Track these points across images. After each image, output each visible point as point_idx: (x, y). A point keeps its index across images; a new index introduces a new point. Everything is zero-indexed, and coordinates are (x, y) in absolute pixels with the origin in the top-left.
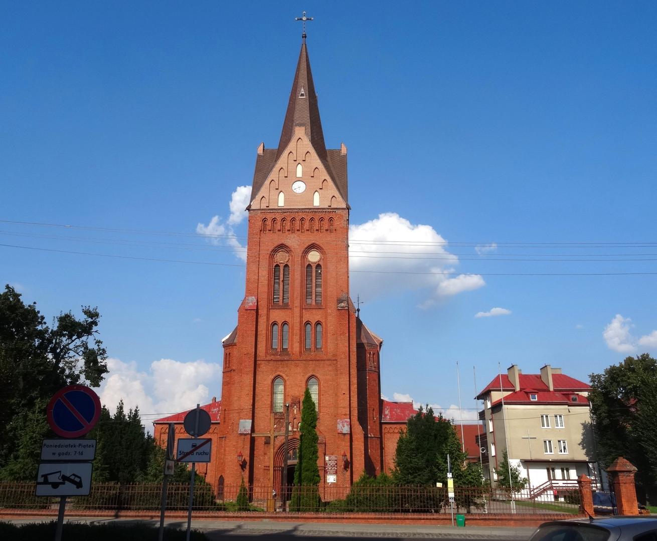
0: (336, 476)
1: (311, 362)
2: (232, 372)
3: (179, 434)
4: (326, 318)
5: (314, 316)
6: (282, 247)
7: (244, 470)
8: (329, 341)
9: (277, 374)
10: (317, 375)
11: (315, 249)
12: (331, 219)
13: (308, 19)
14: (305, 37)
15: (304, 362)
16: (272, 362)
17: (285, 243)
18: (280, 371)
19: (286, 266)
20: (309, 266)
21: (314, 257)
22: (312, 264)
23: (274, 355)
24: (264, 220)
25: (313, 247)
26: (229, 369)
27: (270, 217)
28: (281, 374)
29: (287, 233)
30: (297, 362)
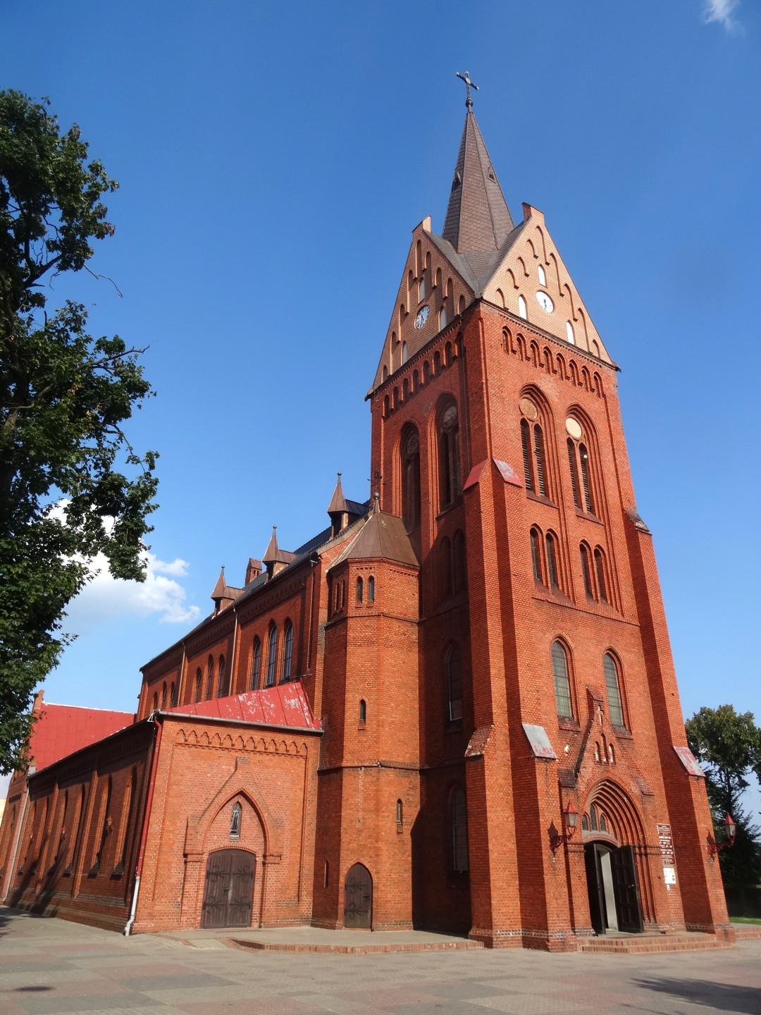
0: (673, 869)
2: (382, 618)
3: (220, 752)
4: (610, 540)
5: (596, 538)
6: (533, 392)
7: (554, 853)
8: (623, 587)
9: (558, 632)
10: (616, 649)
11: (575, 417)
13: (472, 85)
14: (467, 104)
15: (594, 617)
16: (546, 606)
18: (562, 629)
19: (537, 428)
20: (570, 442)
21: (574, 429)
22: (574, 441)
24: (506, 331)
25: (577, 412)
26: (374, 611)
27: (515, 329)
28: (564, 634)
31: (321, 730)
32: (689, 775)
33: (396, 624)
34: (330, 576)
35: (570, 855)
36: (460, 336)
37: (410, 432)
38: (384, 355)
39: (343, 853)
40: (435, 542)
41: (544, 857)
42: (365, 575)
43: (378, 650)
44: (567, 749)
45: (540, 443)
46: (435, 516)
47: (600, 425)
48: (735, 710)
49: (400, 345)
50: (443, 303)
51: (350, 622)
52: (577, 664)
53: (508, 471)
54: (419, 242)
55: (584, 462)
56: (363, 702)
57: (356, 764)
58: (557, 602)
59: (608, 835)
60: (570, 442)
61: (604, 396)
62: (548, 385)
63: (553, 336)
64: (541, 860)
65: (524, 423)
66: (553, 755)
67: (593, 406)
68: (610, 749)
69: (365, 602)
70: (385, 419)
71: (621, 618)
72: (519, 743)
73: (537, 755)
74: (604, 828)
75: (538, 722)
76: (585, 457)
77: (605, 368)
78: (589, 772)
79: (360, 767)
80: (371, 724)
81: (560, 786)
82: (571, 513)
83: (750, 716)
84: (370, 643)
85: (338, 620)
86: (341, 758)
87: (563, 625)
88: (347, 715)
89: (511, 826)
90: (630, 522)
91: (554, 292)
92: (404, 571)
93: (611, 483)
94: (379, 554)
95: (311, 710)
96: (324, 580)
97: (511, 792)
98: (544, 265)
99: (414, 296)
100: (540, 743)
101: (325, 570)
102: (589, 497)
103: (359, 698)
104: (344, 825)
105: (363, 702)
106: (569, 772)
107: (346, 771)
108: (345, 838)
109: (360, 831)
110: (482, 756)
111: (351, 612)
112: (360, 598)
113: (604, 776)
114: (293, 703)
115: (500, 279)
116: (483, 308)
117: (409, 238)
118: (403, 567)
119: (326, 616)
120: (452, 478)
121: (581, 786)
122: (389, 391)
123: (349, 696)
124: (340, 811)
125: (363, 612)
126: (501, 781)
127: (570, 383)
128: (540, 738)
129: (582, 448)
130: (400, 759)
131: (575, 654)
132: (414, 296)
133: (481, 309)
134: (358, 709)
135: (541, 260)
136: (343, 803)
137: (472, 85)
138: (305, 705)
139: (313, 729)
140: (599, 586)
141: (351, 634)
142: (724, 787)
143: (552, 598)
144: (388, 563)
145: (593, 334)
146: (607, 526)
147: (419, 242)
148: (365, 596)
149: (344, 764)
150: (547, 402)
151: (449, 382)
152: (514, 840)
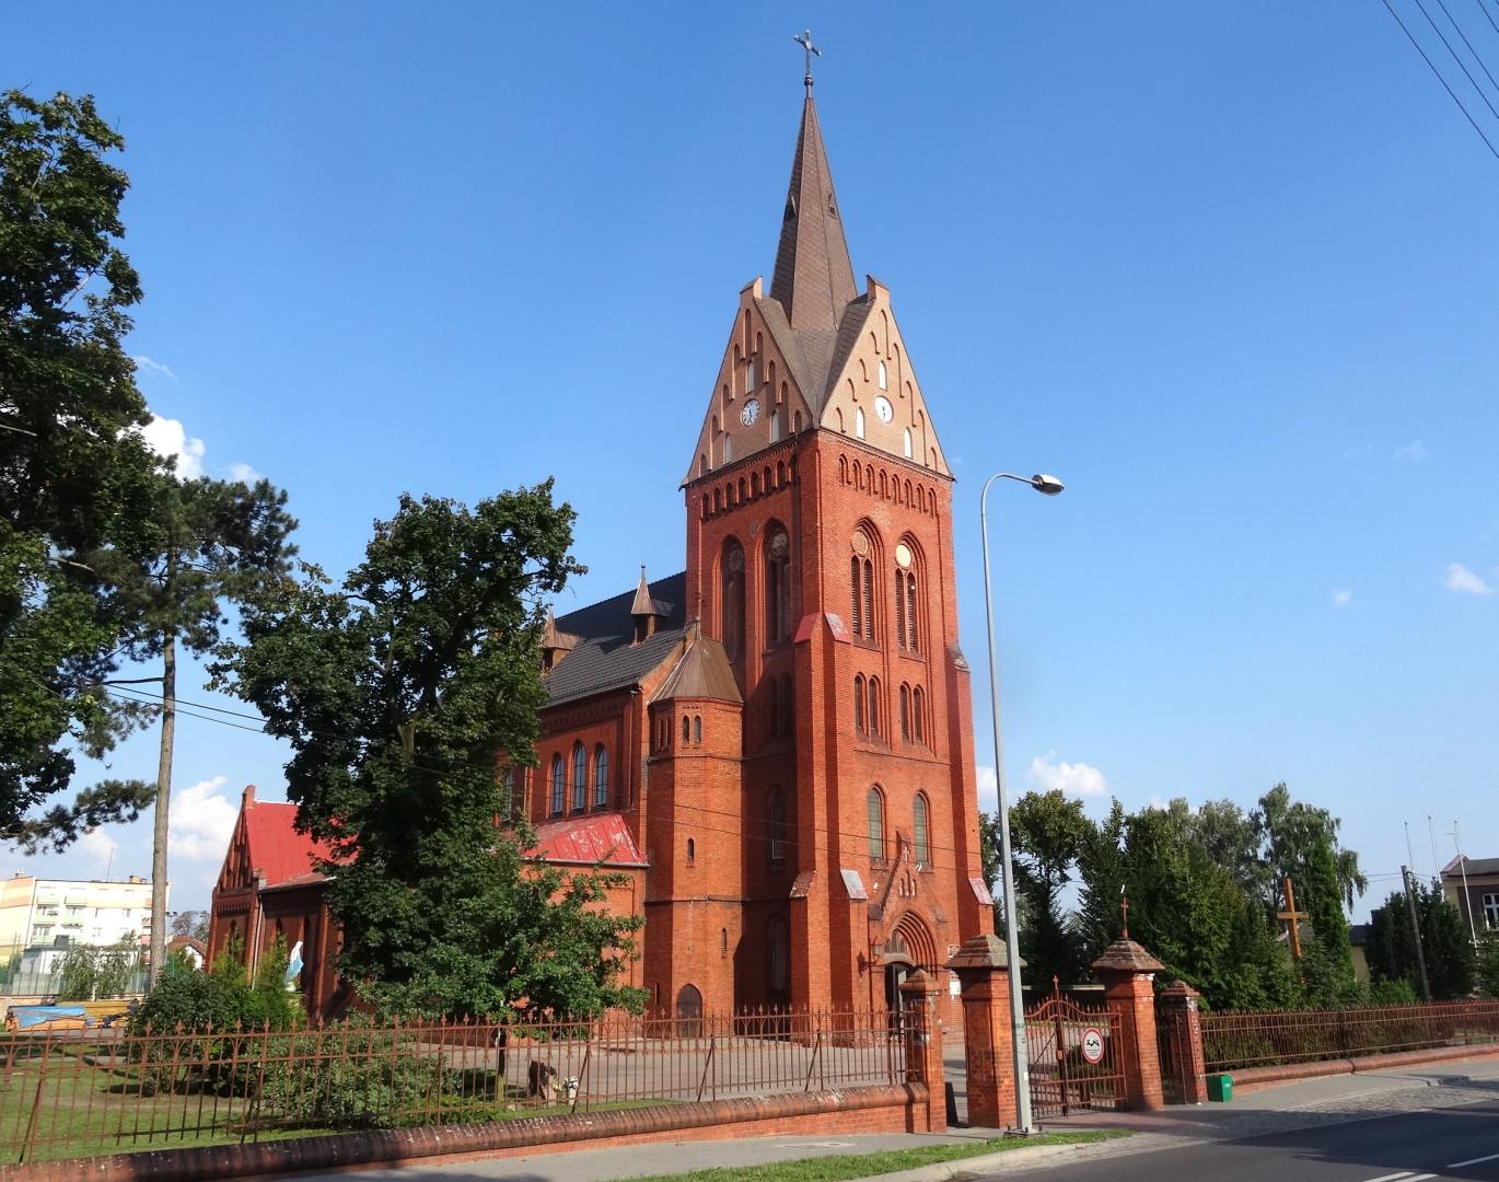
1: (917, 764)
4: (930, 678)
5: (915, 676)
6: (868, 526)
8: (938, 727)
9: (875, 780)
12: (932, 493)
13: (813, 50)
14: (806, 83)
17: (872, 517)
18: (879, 776)
19: (868, 564)
21: (904, 556)
23: (864, 741)
25: (910, 539)
27: (851, 454)
29: (873, 496)
30: (899, 760)
31: (647, 865)
32: (979, 904)
33: (721, 764)
34: (651, 707)
35: (873, 975)
36: (794, 460)
37: (732, 544)
38: (702, 442)
39: (675, 977)
40: (760, 680)
41: (853, 979)
42: (691, 714)
43: (705, 792)
44: (876, 886)
45: (869, 580)
46: (761, 652)
47: (931, 552)
48: (1064, 796)
49: (723, 436)
50: (773, 408)
51: (677, 762)
52: (889, 809)
53: (839, 625)
54: (748, 311)
55: (911, 592)
56: (691, 841)
57: (686, 899)
58: (876, 750)
59: (906, 957)
60: (898, 572)
61: (937, 515)
62: (882, 515)
63: (890, 455)
64: (851, 982)
65: (855, 560)
66: (865, 896)
67: (924, 528)
68: (913, 884)
69: (692, 743)
70: (705, 520)
71: (932, 758)
72: (837, 886)
73: (852, 897)
74: (902, 950)
75: (853, 867)
76: (913, 588)
77: (941, 480)
78: (894, 905)
79: (690, 901)
80: (699, 861)
81: (869, 919)
82: (894, 658)
83: (1079, 804)
84: (697, 784)
85: (663, 759)
86: (672, 892)
87: (880, 772)
88: (676, 853)
89: (827, 954)
90: (950, 656)
91: (894, 395)
92: (728, 708)
93: (935, 616)
94: (705, 693)
95: (636, 845)
96: (645, 713)
97: (828, 926)
98: (886, 361)
99: (741, 380)
100: (854, 886)
101: (646, 703)
102: (914, 631)
103: (687, 838)
104: (675, 952)
105: (691, 841)
106: (876, 907)
107: (675, 904)
108: (676, 964)
109: (690, 957)
110: (805, 897)
111: (678, 753)
112: (686, 735)
113: (907, 907)
114: (618, 837)
115: (840, 396)
116: (822, 437)
117: (734, 304)
118: (729, 705)
119: (648, 750)
120: (780, 614)
121: (886, 918)
122: (709, 489)
123: (677, 835)
124: (671, 940)
125: (691, 752)
126: (821, 918)
127: (903, 507)
128: (854, 881)
129: (911, 577)
130: (725, 893)
131: (889, 799)
132: (741, 380)
133: (819, 439)
134: (686, 848)
135: (883, 356)
136: (674, 933)
137: (813, 50)
138: (629, 838)
139: (640, 864)
140: (916, 726)
141: (678, 775)
142: (1043, 882)
143: (872, 747)
144: (716, 702)
145: (931, 441)
146: (929, 664)
147: (748, 311)
148: (691, 736)
149: (674, 898)
150: (879, 534)
151: (779, 506)
152: (829, 966)
